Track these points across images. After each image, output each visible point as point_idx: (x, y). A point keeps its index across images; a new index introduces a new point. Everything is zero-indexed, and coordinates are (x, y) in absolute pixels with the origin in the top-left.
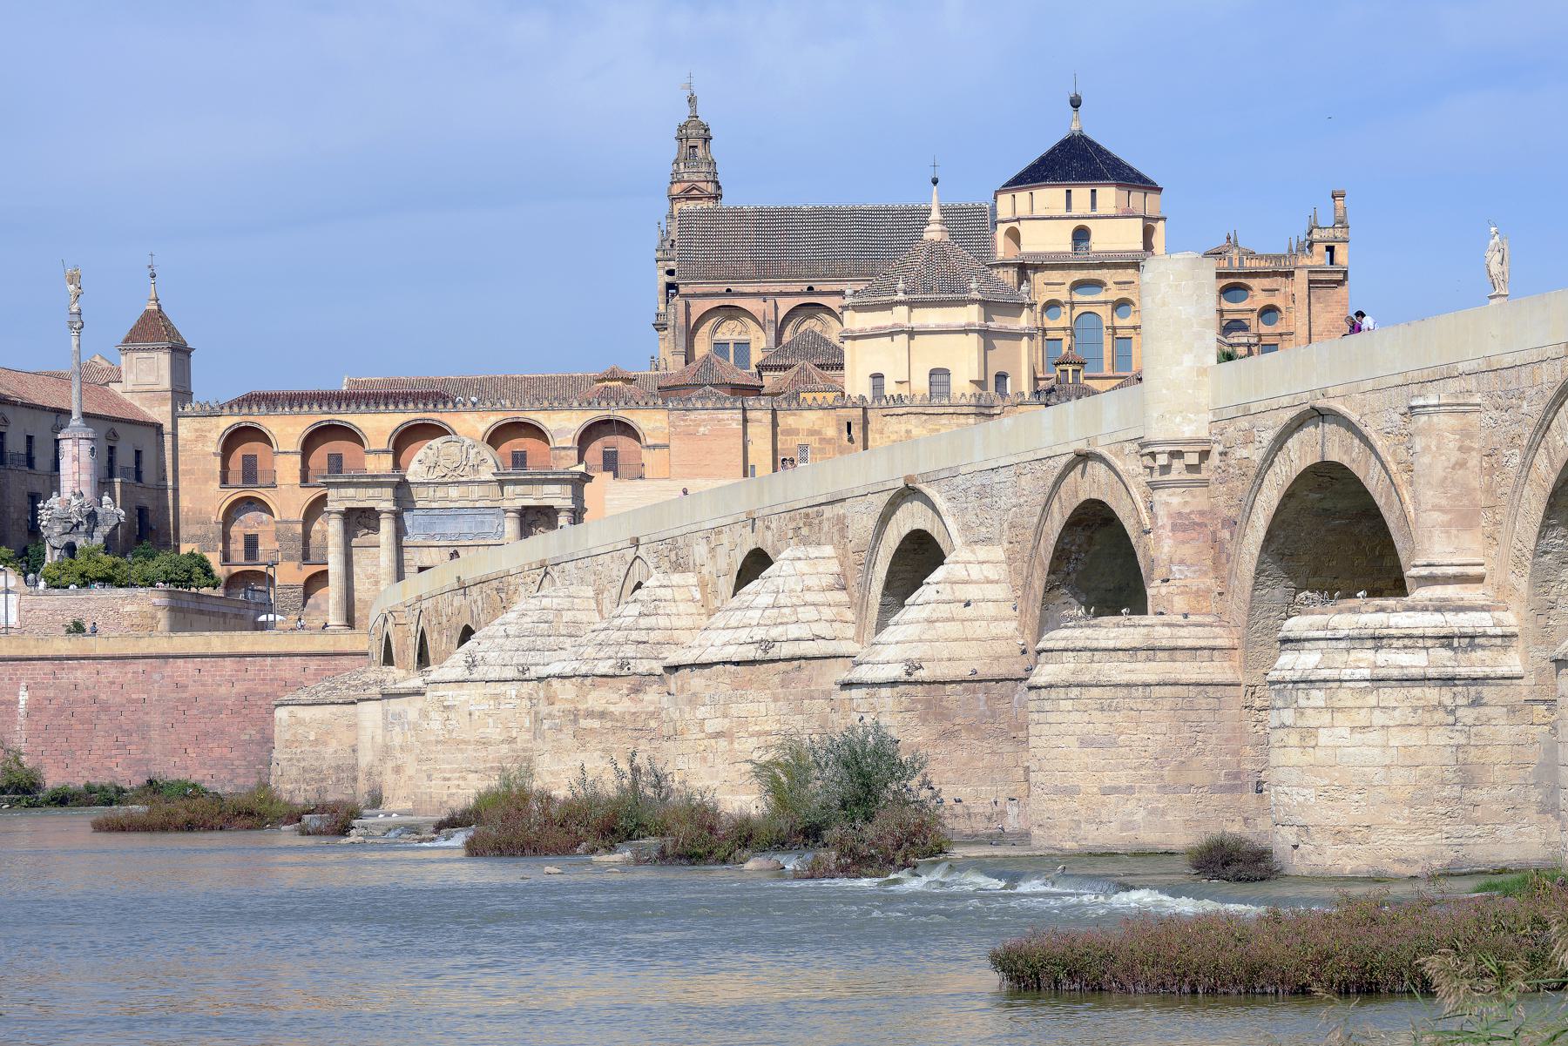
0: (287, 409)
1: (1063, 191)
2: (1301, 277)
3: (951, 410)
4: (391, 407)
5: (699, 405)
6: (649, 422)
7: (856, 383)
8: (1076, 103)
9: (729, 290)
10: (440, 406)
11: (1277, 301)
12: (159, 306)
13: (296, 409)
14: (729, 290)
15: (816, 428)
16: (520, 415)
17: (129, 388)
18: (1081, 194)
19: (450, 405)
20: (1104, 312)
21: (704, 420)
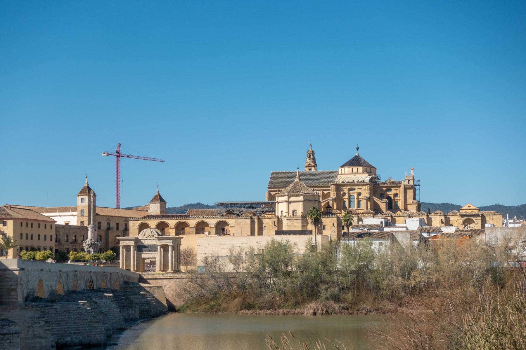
0: (153, 219)
1: (351, 168)
3: (296, 219)
4: (175, 218)
5: (241, 218)
6: (231, 221)
7: (279, 214)
9: (279, 190)
10: (186, 218)
11: (398, 192)
12: (159, 193)
13: (155, 219)
14: (279, 190)
15: (268, 223)
16: (203, 220)
17: (152, 211)
18: (355, 169)
19: (188, 218)
20: (355, 195)
21: (242, 221)
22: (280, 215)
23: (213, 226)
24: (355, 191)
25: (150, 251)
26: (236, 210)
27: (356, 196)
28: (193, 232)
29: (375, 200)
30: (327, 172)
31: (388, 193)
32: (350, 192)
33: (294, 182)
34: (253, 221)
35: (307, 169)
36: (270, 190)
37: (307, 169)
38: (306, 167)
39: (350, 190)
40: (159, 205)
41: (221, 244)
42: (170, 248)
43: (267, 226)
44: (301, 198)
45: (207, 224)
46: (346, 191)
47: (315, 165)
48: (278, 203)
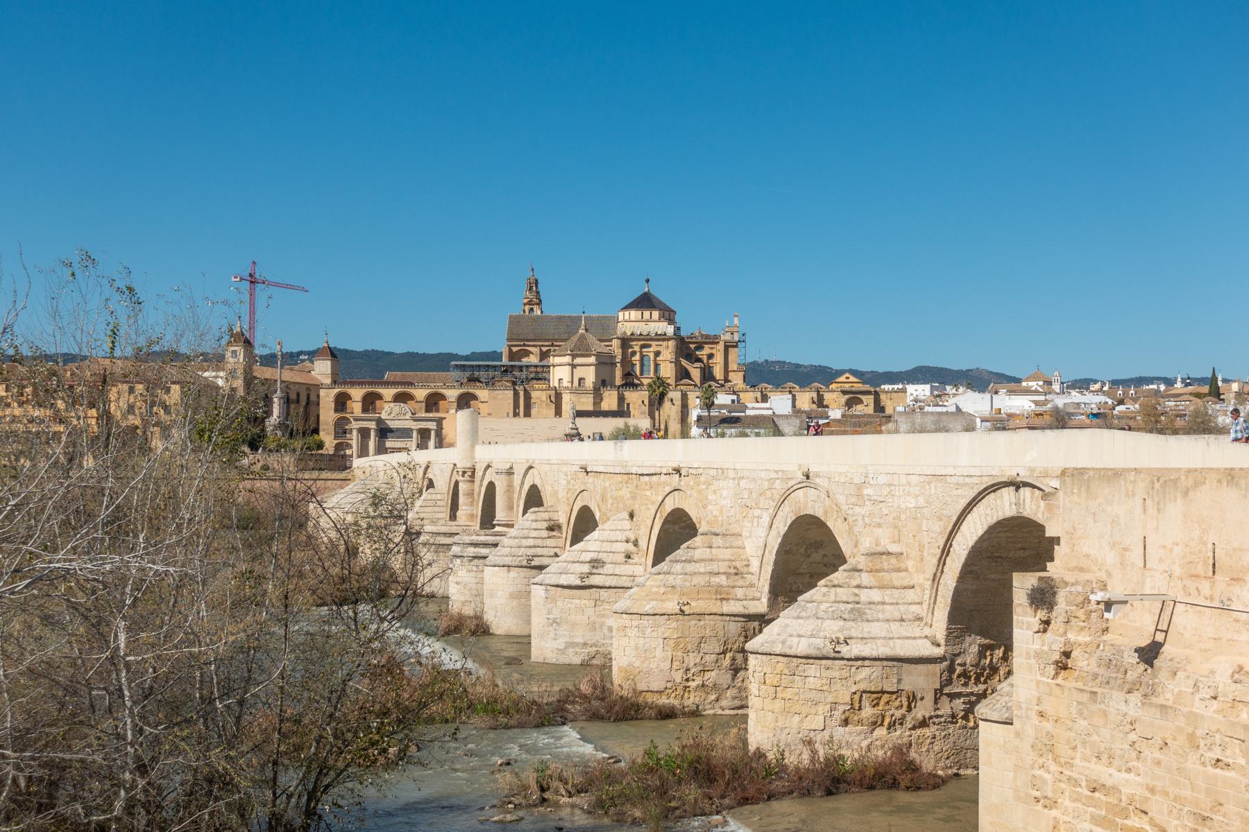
2: (721, 346)
7: (554, 383)
8: (648, 281)
18: (647, 314)
20: (652, 356)
22: (557, 386)
23: (453, 399)
24: (651, 349)
25: (399, 438)
26: (483, 375)
27: (652, 358)
28: (421, 408)
29: (683, 363)
30: (598, 318)
31: (697, 353)
32: (643, 350)
33: (578, 335)
34: (516, 394)
35: (527, 308)
36: (511, 343)
37: (527, 308)
38: (525, 304)
39: (643, 347)
40: (329, 363)
41: (492, 429)
42: (373, 434)
43: (538, 401)
44: (592, 360)
45: (443, 397)
46: (637, 348)
47: (540, 303)
48: (554, 366)
